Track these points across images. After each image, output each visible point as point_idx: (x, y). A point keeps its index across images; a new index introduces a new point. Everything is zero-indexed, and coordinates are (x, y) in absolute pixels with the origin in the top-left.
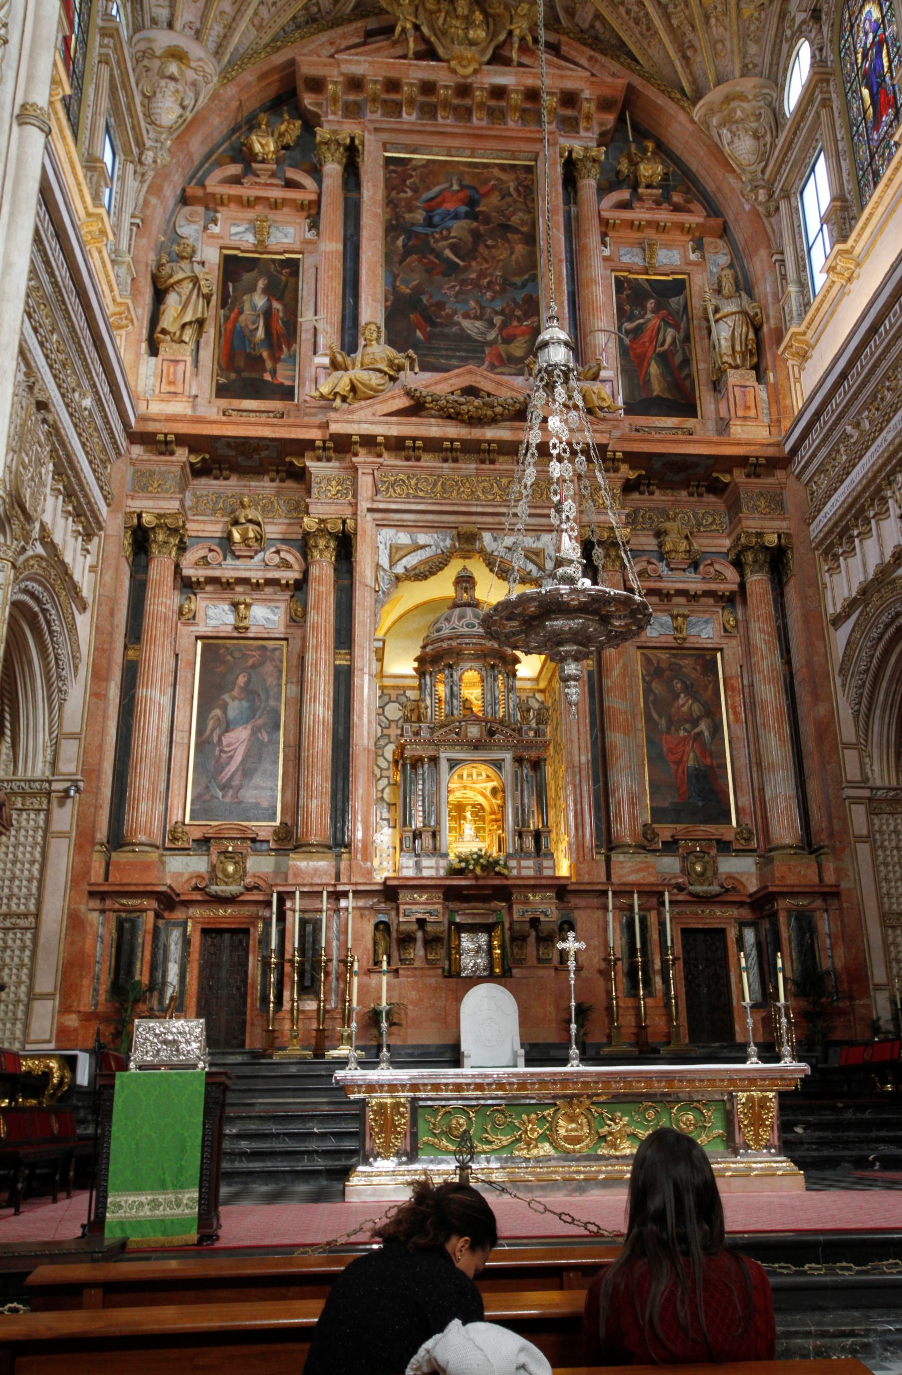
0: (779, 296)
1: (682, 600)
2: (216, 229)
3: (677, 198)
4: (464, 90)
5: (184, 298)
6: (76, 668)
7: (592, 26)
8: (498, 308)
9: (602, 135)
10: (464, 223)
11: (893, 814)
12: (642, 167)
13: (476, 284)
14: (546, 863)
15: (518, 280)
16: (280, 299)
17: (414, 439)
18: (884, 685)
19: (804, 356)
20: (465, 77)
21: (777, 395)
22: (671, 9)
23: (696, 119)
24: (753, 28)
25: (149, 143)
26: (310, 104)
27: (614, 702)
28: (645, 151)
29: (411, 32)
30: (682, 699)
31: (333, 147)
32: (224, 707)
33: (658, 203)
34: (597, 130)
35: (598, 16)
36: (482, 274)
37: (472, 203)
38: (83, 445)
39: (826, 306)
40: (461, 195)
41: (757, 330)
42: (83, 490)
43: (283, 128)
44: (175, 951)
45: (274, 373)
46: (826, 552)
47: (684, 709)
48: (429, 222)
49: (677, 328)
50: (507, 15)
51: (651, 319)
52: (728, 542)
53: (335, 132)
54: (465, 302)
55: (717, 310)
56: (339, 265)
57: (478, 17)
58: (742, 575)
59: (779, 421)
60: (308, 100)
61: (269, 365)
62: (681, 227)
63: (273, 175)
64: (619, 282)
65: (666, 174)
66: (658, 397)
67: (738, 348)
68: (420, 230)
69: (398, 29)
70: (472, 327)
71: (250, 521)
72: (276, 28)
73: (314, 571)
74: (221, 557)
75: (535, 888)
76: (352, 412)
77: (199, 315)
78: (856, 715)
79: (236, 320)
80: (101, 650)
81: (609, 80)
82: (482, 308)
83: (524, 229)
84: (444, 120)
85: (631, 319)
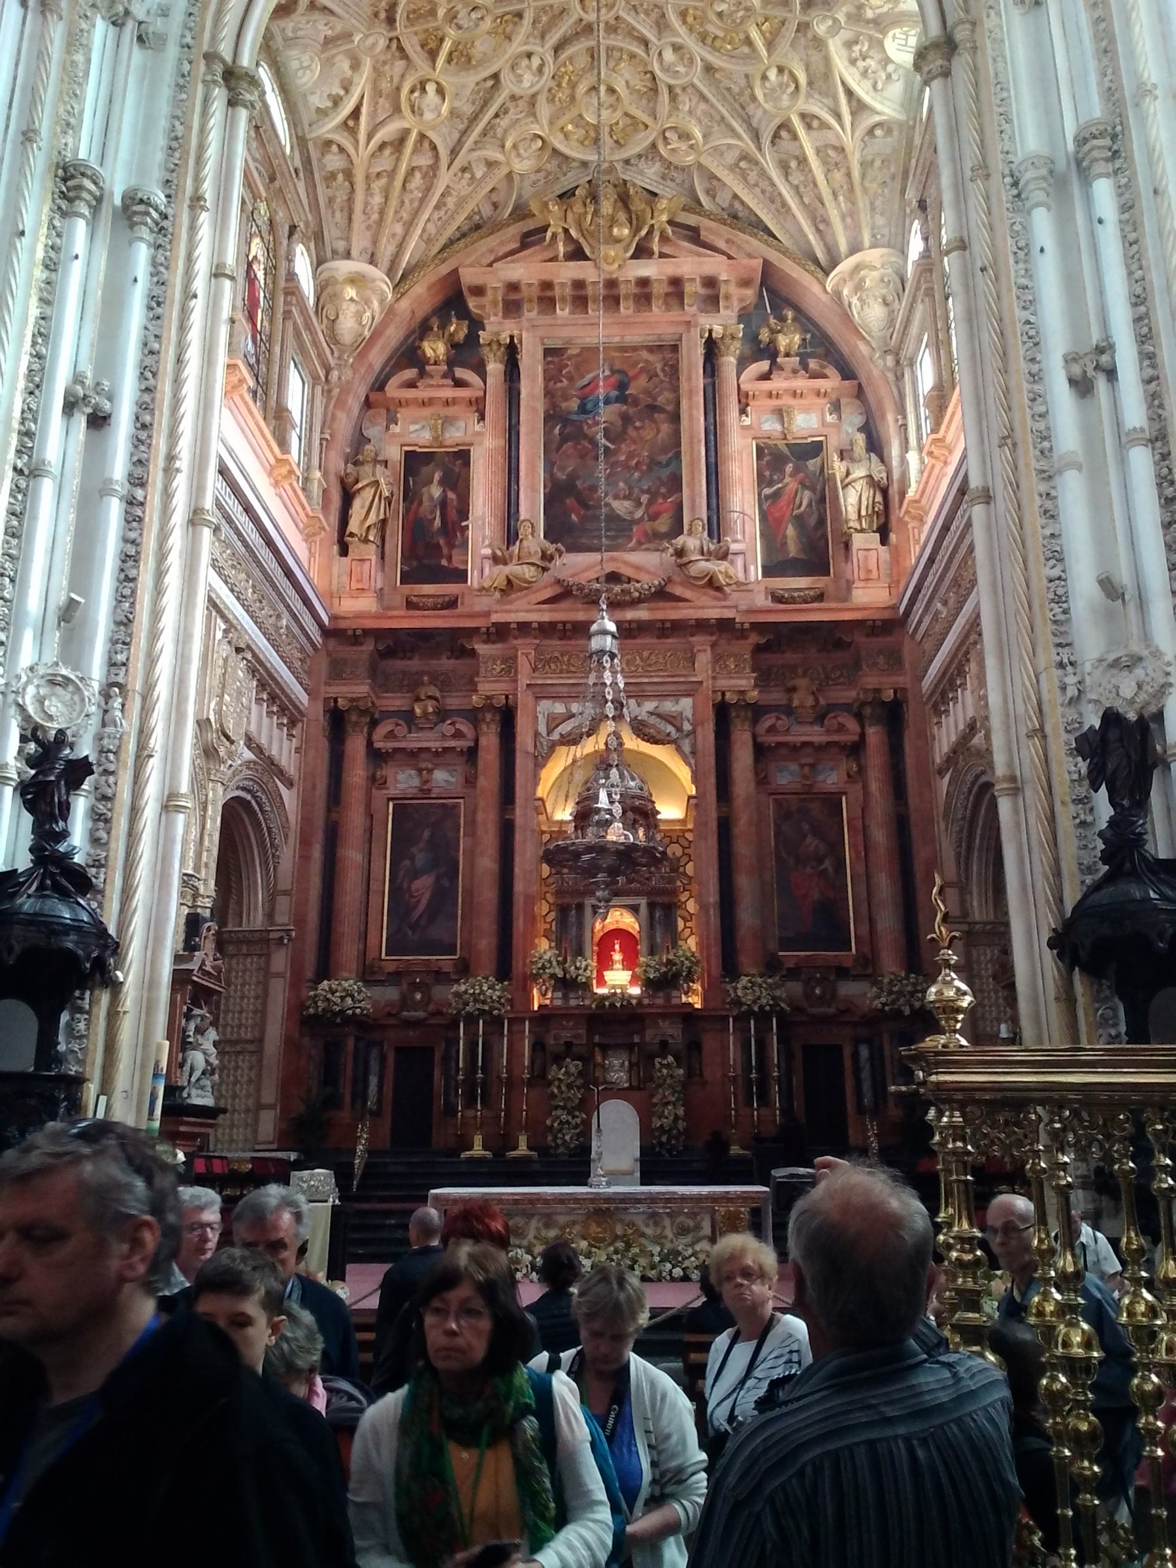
0: (903, 462)
1: (809, 750)
2: (396, 429)
3: (813, 364)
4: (612, 284)
5: (367, 504)
6: (286, 837)
7: (731, 205)
8: (645, 487)
9: (744, 308)
10: (616, 407)
11: (989, 946)
12: (780, 337)
13: (626, 467)
14: (675, 993)
15: (663, 458)
16: (454, 489)
17: (564, 623)
18: (979, 831)
19: (921, 521)
20: (611, 273)
21: (897, 557)
22: (802, 189)
23: (829, 289)
24: (878, 203)
25: (332, 362)
26: (476, 307)
27: (743, 849)
28: (782, 319)
29: (561, 236)
30: (809, 839)
31: (495, 347)
32: (412, 859)
33: (795, 372)
34: (736, 307)
35: (735, 196)
36: (631, 456)
37: (622, 386)
38: (281, 657)
39: (932, 481)
40: (613, 380)
41: (885, 492)
42: (283, 691)
43: (452, 329)
44: (374, 1066)
45: (450, 559)
46: (935, 706)
47: (812, 848)
48: (583, 409)
49: (813, 489)
50: (649, 212)
51: (790, 483)
52: (853, 694)
53: (498, 334)
54: (616, 484)
55: (848, 474)
56: (501, 459)
57: (622, 216)
58: (863, 727)
59: (898, 581)
60: (472, 303)
61: (445, 551)
62: (818, 394)
63: (444, 376)
64: (758, 448)
65: (804, 340)
66: (795, 559)
67: (863, 513)
68: (575, 417)
69: (549, 234)
70: (621, 507)
71: (430, 697)
72: (442, 241)
73: (483, 741)
74: (406, 730)
75: (664, 1016)
76: (511, 603)
77: (382, 516)
78: (958, 855)
79: (416, 513)
80: (306, 820)
81: (746, 261)
82: (630, 488)
83: (670, 408)
84: (596, 312)
85: (770, 484)
